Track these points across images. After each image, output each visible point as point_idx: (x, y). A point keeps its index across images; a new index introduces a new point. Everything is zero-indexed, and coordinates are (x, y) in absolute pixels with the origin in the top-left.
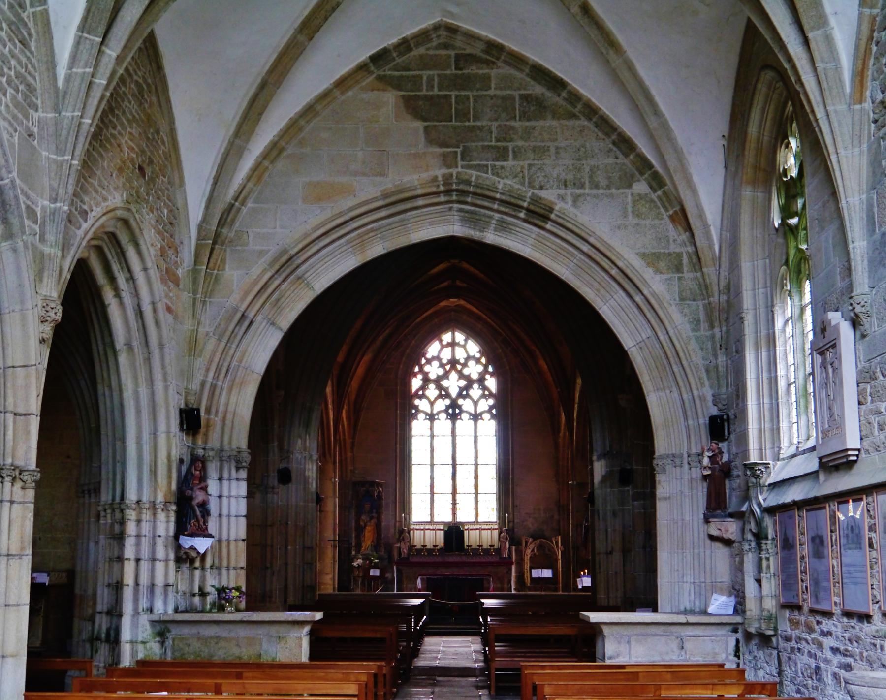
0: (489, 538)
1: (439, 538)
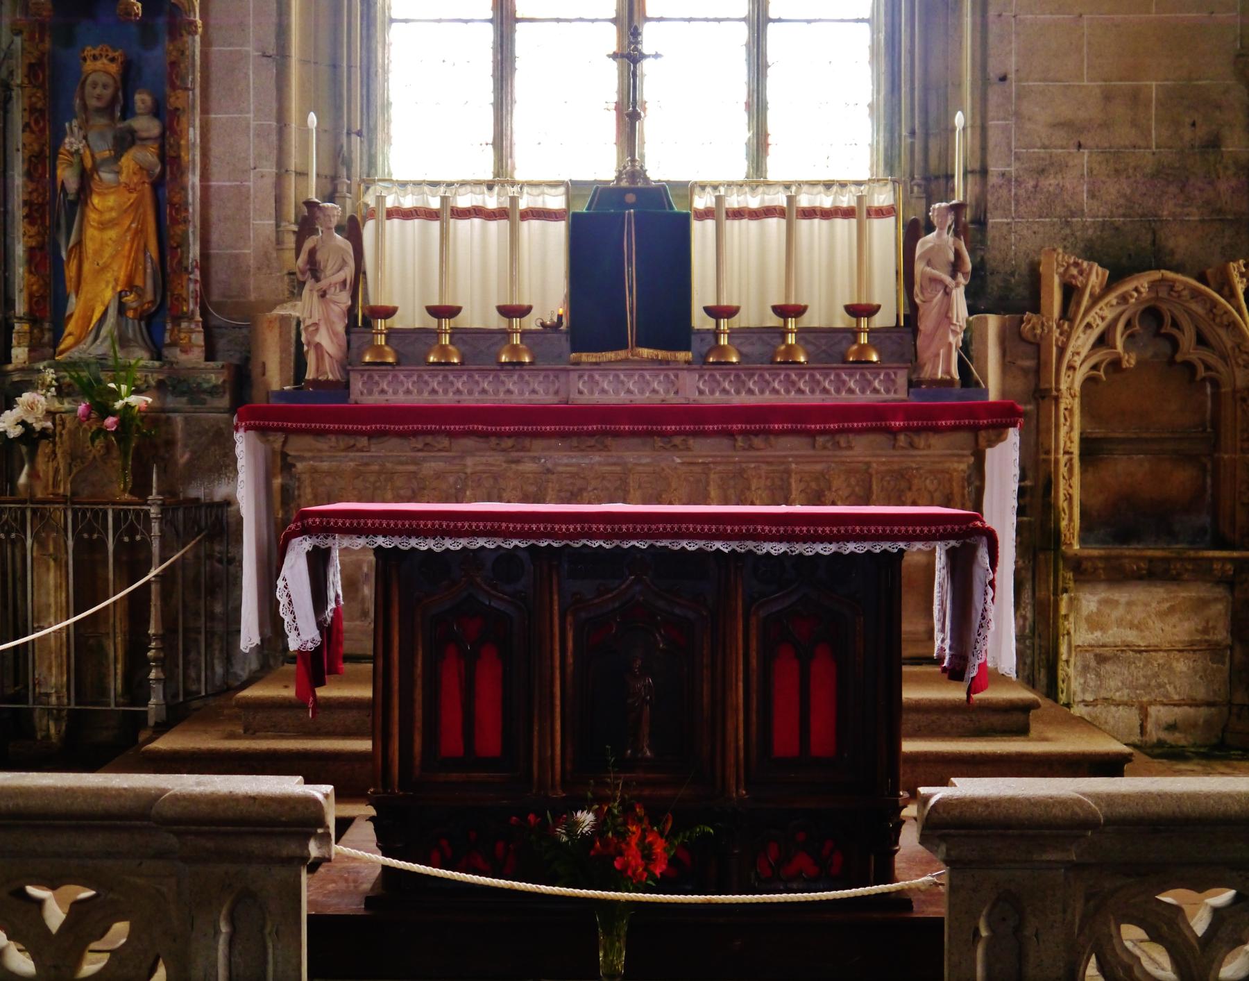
0: (847, 273)
1: (548, 291)
